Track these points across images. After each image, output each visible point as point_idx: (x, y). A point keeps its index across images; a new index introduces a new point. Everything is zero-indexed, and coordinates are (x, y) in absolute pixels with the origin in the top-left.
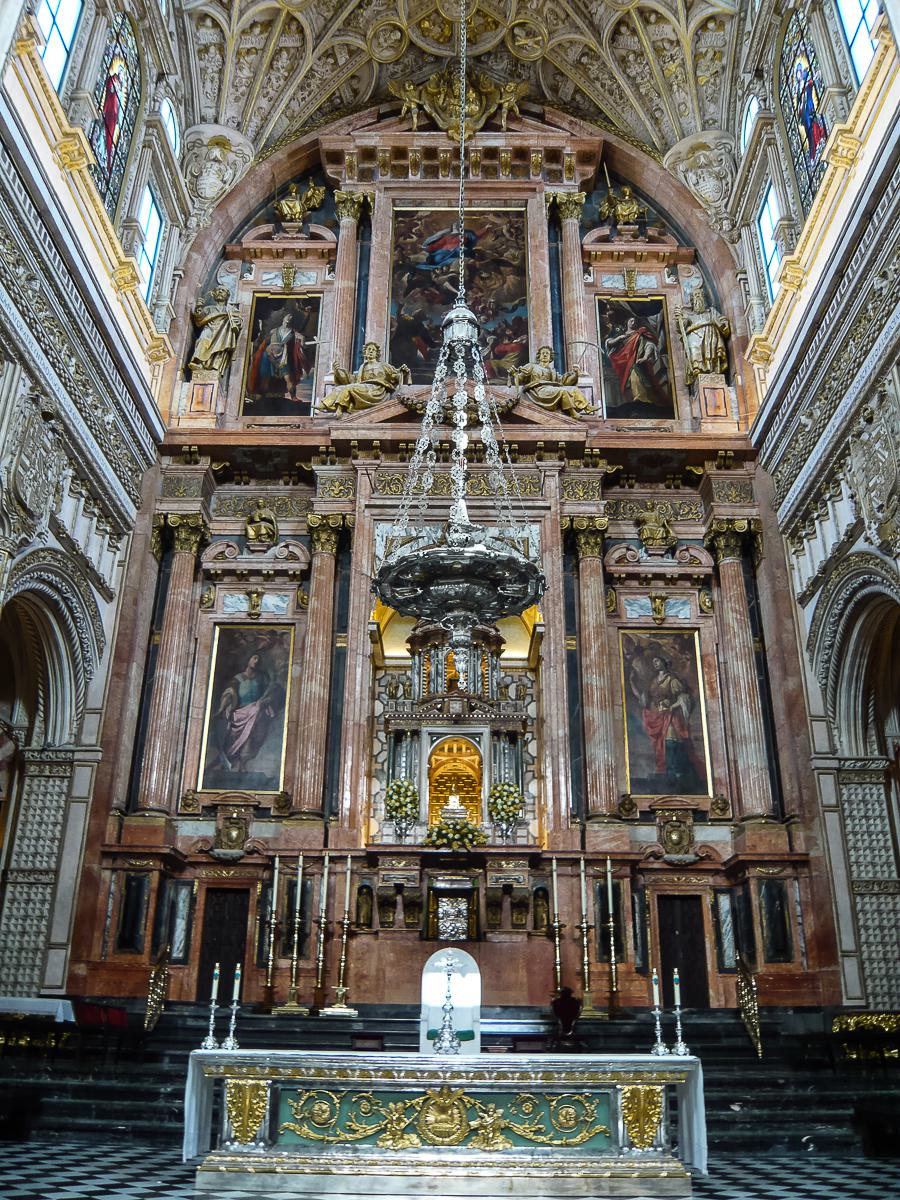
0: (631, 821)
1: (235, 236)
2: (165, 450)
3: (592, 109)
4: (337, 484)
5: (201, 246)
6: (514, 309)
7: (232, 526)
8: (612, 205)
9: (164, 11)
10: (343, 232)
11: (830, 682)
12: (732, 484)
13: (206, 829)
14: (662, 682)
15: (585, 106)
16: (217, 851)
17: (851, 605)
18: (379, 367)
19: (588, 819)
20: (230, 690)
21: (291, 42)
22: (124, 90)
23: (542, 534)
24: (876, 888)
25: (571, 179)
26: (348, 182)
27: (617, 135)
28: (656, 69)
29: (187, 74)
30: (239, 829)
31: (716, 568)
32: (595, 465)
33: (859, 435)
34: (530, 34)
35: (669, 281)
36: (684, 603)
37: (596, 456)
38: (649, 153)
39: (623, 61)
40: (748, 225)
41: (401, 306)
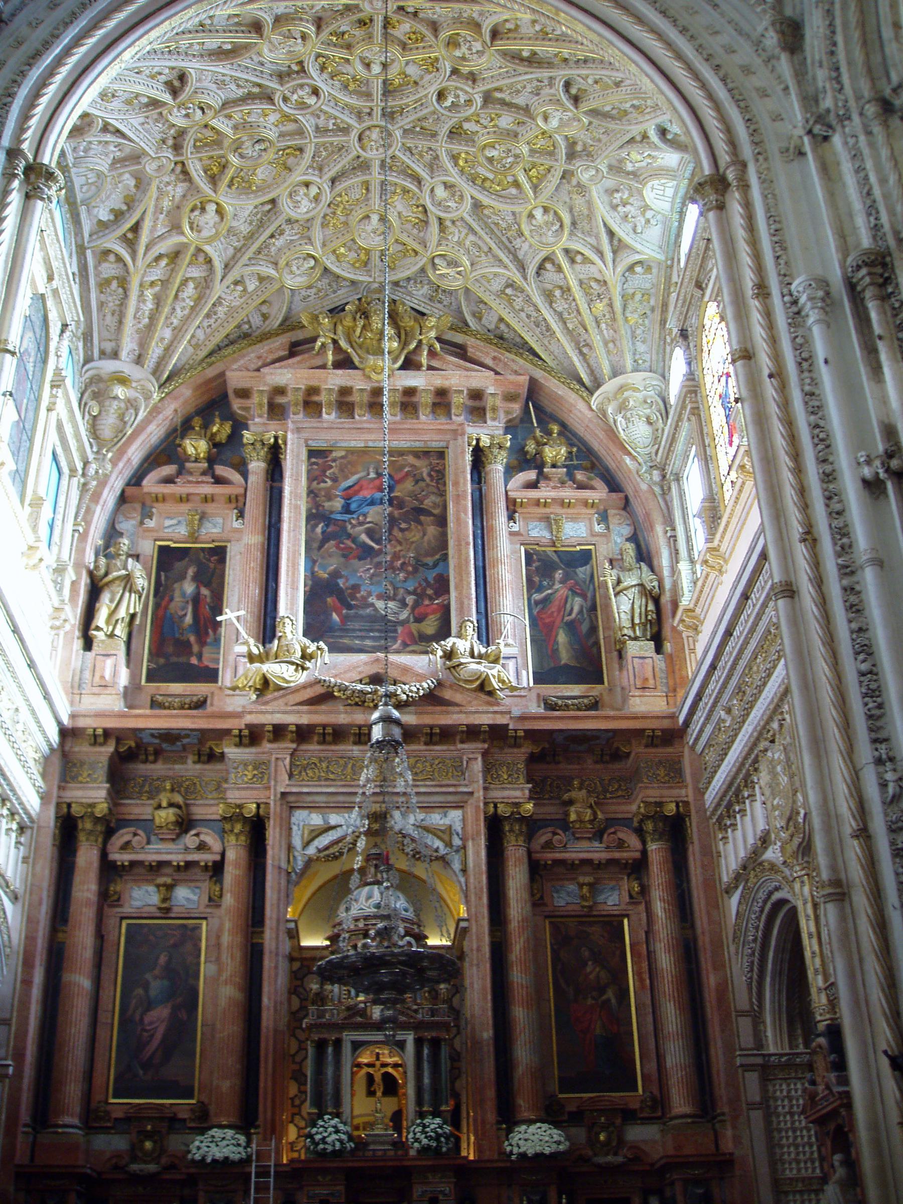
1: (136, 480)
3: (518, 340)
4: (250, 768)
5: (101, 493)
6: (435, 565)
10: (252, 479)
12: (660, 762)
13: (118, 1143)
14: (591, 972)
20: (140, 991)
22: (31, 360)
23: (464, 820)
24: (800, 1185)
25: (494, 419)
26: (257, 420)
27: (545, 370)
30: (155, 1142)
31: (644, 852)
32: (519, 746)
33: (766, 750)
34: (453, 263)
35: (598, 528)
36: (613, 889)
37: (520, 737)
39: (549, 296)
40: (678, 479)
41: (314, 562)
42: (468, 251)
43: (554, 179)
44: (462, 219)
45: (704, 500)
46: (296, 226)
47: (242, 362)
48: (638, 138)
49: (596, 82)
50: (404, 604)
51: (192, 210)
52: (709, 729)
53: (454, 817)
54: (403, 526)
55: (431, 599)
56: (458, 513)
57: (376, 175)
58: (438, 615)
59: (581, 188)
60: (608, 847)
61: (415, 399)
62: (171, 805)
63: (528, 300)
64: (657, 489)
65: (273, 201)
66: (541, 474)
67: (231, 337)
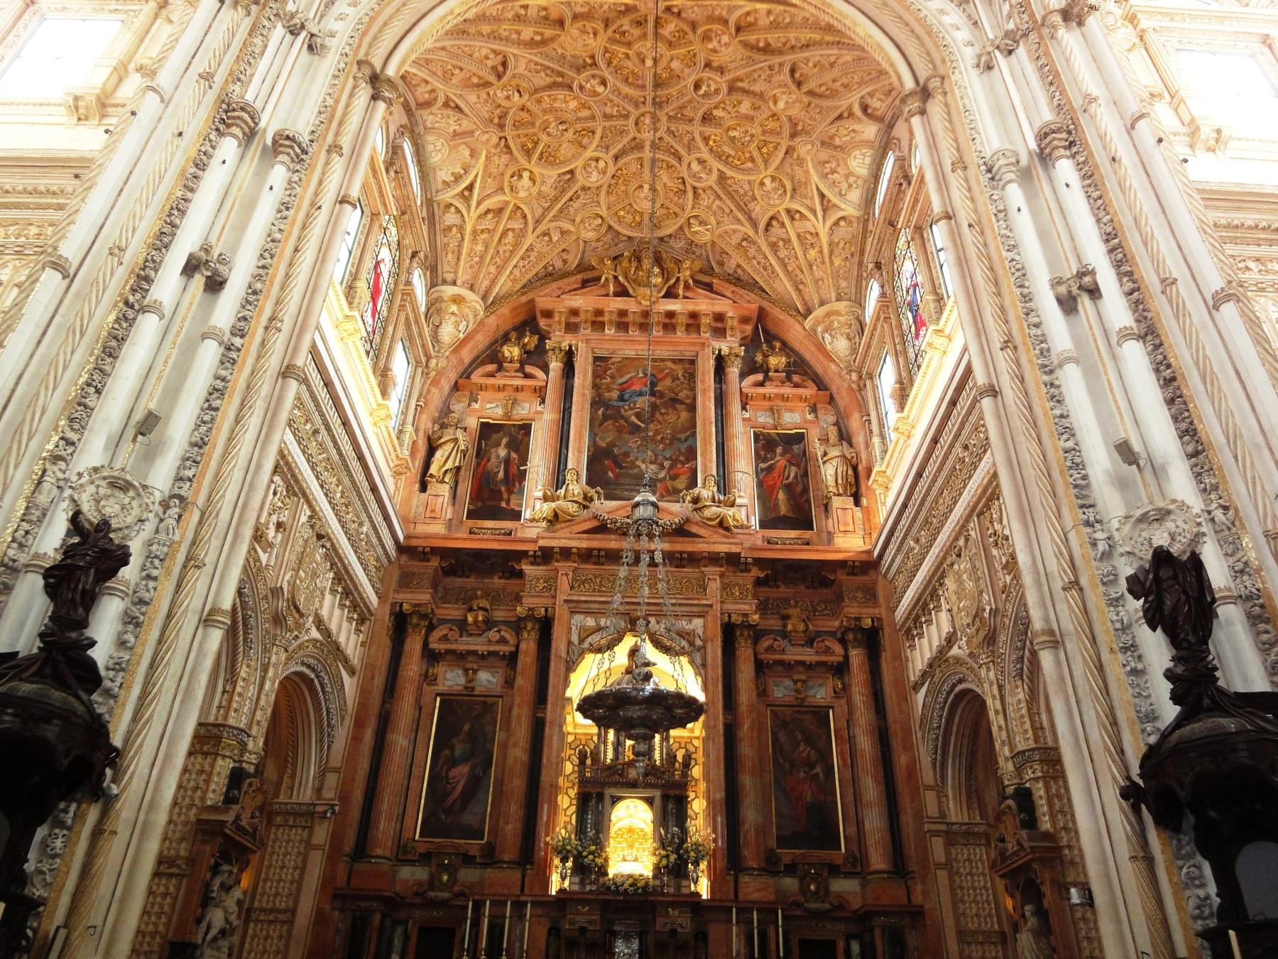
0: (775, 873)
1: (467, 374)
2: (401, 549)
7: (452, 611)
8: (766, 356)
10: (551, 374)
11: (939, 757)
13: (421, 873)
15: (745, 278)
16: (432, 894)
17: (952, 696)
18: (576, 487)
19: (742, 870)
20: (447, 752)
21: (517, 225)
23: (704, 626)
24: (981, 939)
28: (800, 254)
29: (433, 246)
30: (450, 874)
31: (846, 657)
32: (748, 571)
33: (952, 564)
34: (702, 223)
35: (810, 417)
39: (774, 247)
40: (871, 378)
42: (715, 214)
43: (781, 155)
48: (846, 115)
49: (815, 66)
53: (698, 623)
55: (683, 463)
56: (704, 401)
57: (647, 154)
59: (801, 161)
61: (674, 321)
64: (854, 386)
65: (572, 172)
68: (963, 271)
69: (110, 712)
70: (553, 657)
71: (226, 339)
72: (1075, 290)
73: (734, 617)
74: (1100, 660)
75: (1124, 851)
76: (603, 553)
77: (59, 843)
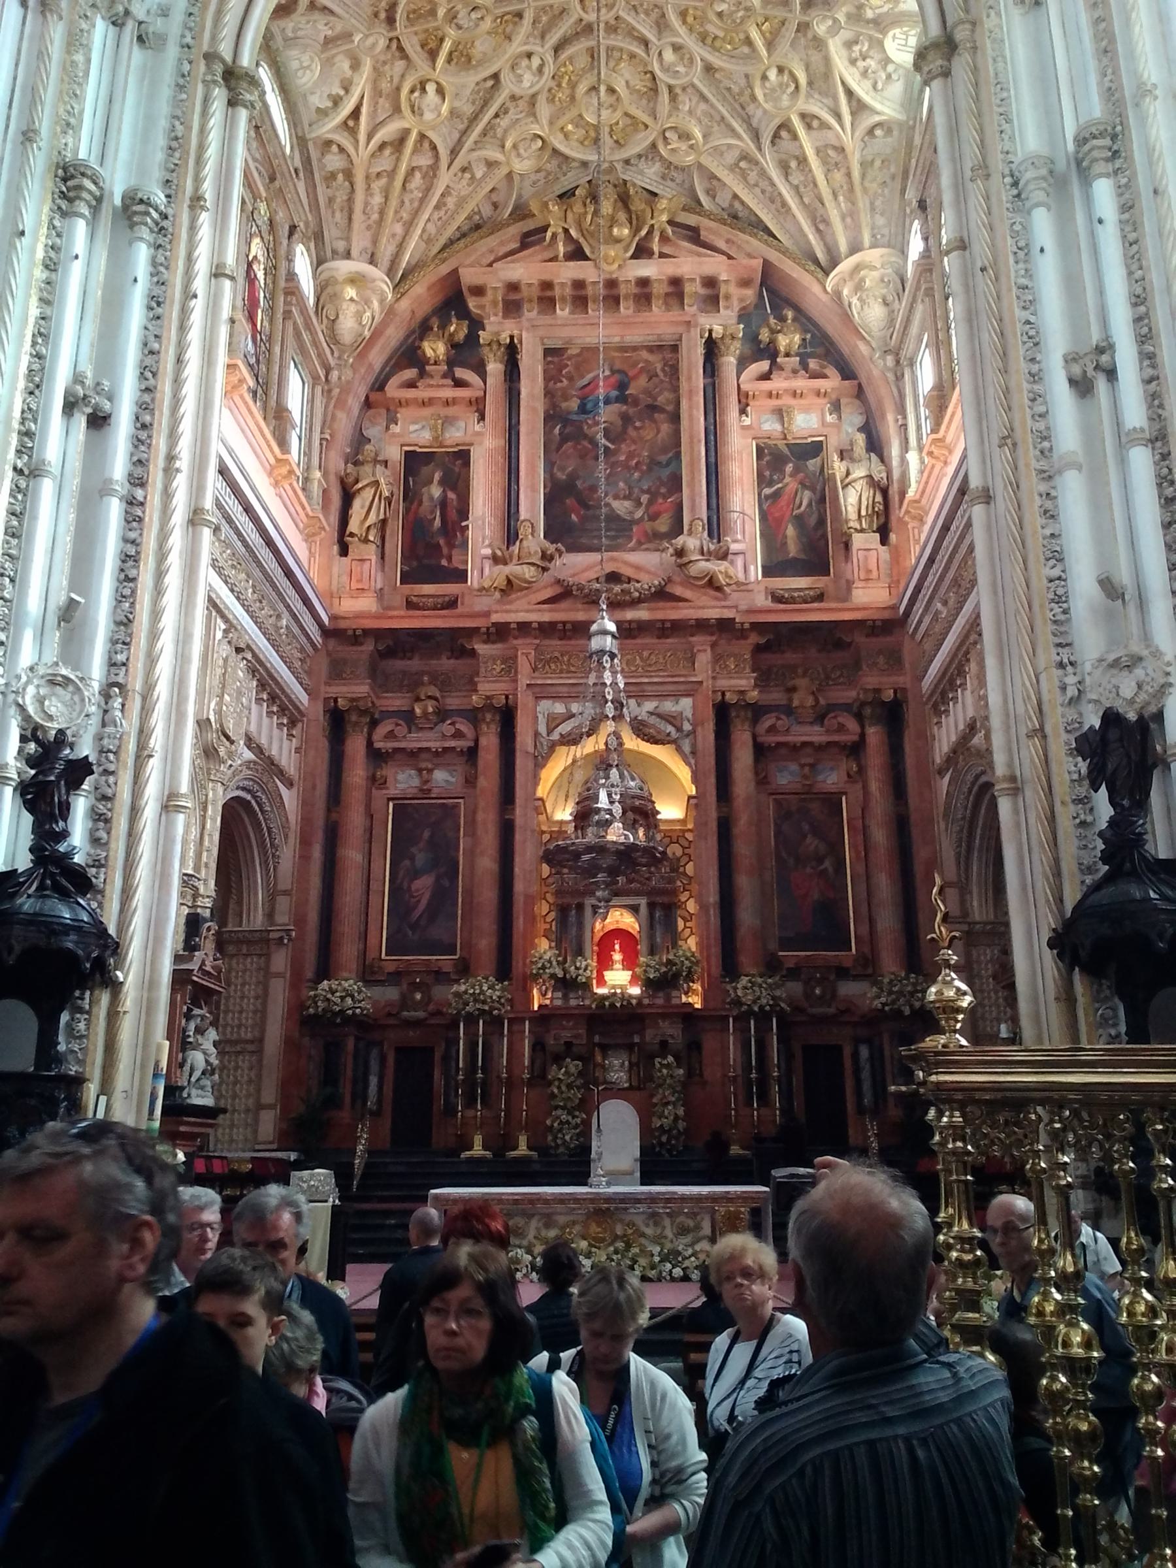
1: (379, 385)
3: (753, 218)
6: (668, 464)
7: (396, 701)
8: (774, 332)
9: (288, 150)
17: (976, 788)
18: (534, 541)
20: (407, 863)
21: (425, 161)
23: (694, 707)
25: (727, 308)
31: (863, 735)
32: (746, 638)
35: (829, 418)
36: (832, 769)
38: (812, 273)
39: (785, 168)
40: (912, 364)
43: (789, 32)
44: (693, 86)
45: (933, 389)
46: (521, 103)
47: (473, 258)
50: (638, 504)
51: (412, 91)
52: (927, 620)
53: (686, 704)
54: (638, 424)
56: (691, 408)
58: (670, 514)
59: (819, 44)
60: (827, 731)
62: (430, 697)
63: (763, 173)
65: (496, 76)
66: (774, 363)
67: (465, 228)
68: (971, 327)
69: (100, 905)
70: (518, 754)
71: (125, 492)
72: (1090, 372)
73: (728, 696)
74: (1053, 812)
75: (1052, 993)
76: (568, 626)
77: (82, 1026)
